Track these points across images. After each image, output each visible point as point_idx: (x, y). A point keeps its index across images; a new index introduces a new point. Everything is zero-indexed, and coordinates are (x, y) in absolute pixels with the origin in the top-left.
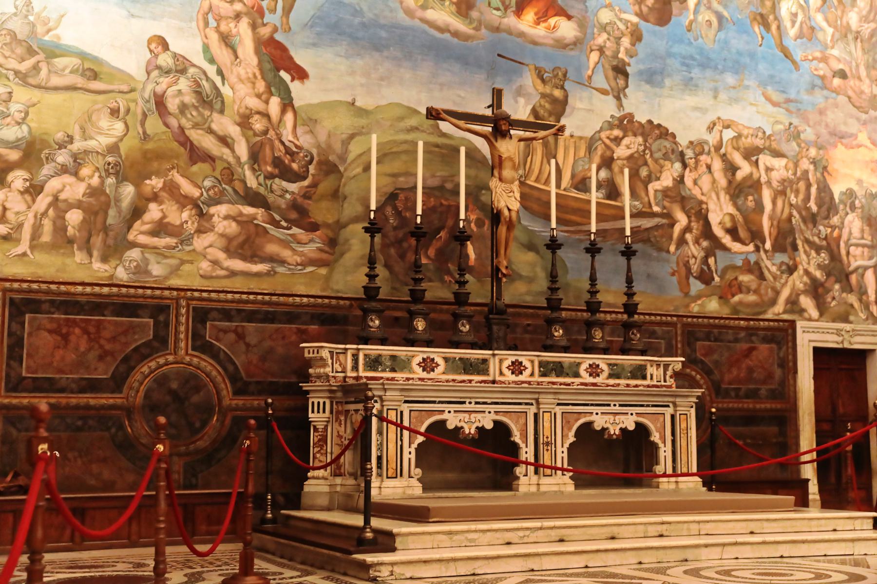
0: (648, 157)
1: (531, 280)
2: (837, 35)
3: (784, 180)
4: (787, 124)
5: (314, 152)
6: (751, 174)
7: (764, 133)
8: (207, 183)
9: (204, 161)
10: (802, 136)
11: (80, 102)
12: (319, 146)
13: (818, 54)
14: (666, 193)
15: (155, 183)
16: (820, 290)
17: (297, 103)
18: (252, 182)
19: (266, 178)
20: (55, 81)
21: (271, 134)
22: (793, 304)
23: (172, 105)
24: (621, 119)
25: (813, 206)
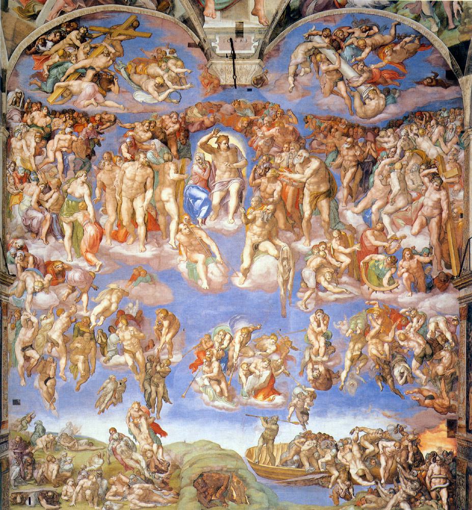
1: (260, 503)
4: (396, 425)
6: (374, 450)
8: (131, 477)
10: (405, 430)
11: (89, 454)
13: (416, 390)
14: (327, 463)
15: (114, 479)
16: (413, 500)
18: (147, 474)
20: (80, 448)
21: (154, 457)
23: (119, 451)
25: (410, 462)
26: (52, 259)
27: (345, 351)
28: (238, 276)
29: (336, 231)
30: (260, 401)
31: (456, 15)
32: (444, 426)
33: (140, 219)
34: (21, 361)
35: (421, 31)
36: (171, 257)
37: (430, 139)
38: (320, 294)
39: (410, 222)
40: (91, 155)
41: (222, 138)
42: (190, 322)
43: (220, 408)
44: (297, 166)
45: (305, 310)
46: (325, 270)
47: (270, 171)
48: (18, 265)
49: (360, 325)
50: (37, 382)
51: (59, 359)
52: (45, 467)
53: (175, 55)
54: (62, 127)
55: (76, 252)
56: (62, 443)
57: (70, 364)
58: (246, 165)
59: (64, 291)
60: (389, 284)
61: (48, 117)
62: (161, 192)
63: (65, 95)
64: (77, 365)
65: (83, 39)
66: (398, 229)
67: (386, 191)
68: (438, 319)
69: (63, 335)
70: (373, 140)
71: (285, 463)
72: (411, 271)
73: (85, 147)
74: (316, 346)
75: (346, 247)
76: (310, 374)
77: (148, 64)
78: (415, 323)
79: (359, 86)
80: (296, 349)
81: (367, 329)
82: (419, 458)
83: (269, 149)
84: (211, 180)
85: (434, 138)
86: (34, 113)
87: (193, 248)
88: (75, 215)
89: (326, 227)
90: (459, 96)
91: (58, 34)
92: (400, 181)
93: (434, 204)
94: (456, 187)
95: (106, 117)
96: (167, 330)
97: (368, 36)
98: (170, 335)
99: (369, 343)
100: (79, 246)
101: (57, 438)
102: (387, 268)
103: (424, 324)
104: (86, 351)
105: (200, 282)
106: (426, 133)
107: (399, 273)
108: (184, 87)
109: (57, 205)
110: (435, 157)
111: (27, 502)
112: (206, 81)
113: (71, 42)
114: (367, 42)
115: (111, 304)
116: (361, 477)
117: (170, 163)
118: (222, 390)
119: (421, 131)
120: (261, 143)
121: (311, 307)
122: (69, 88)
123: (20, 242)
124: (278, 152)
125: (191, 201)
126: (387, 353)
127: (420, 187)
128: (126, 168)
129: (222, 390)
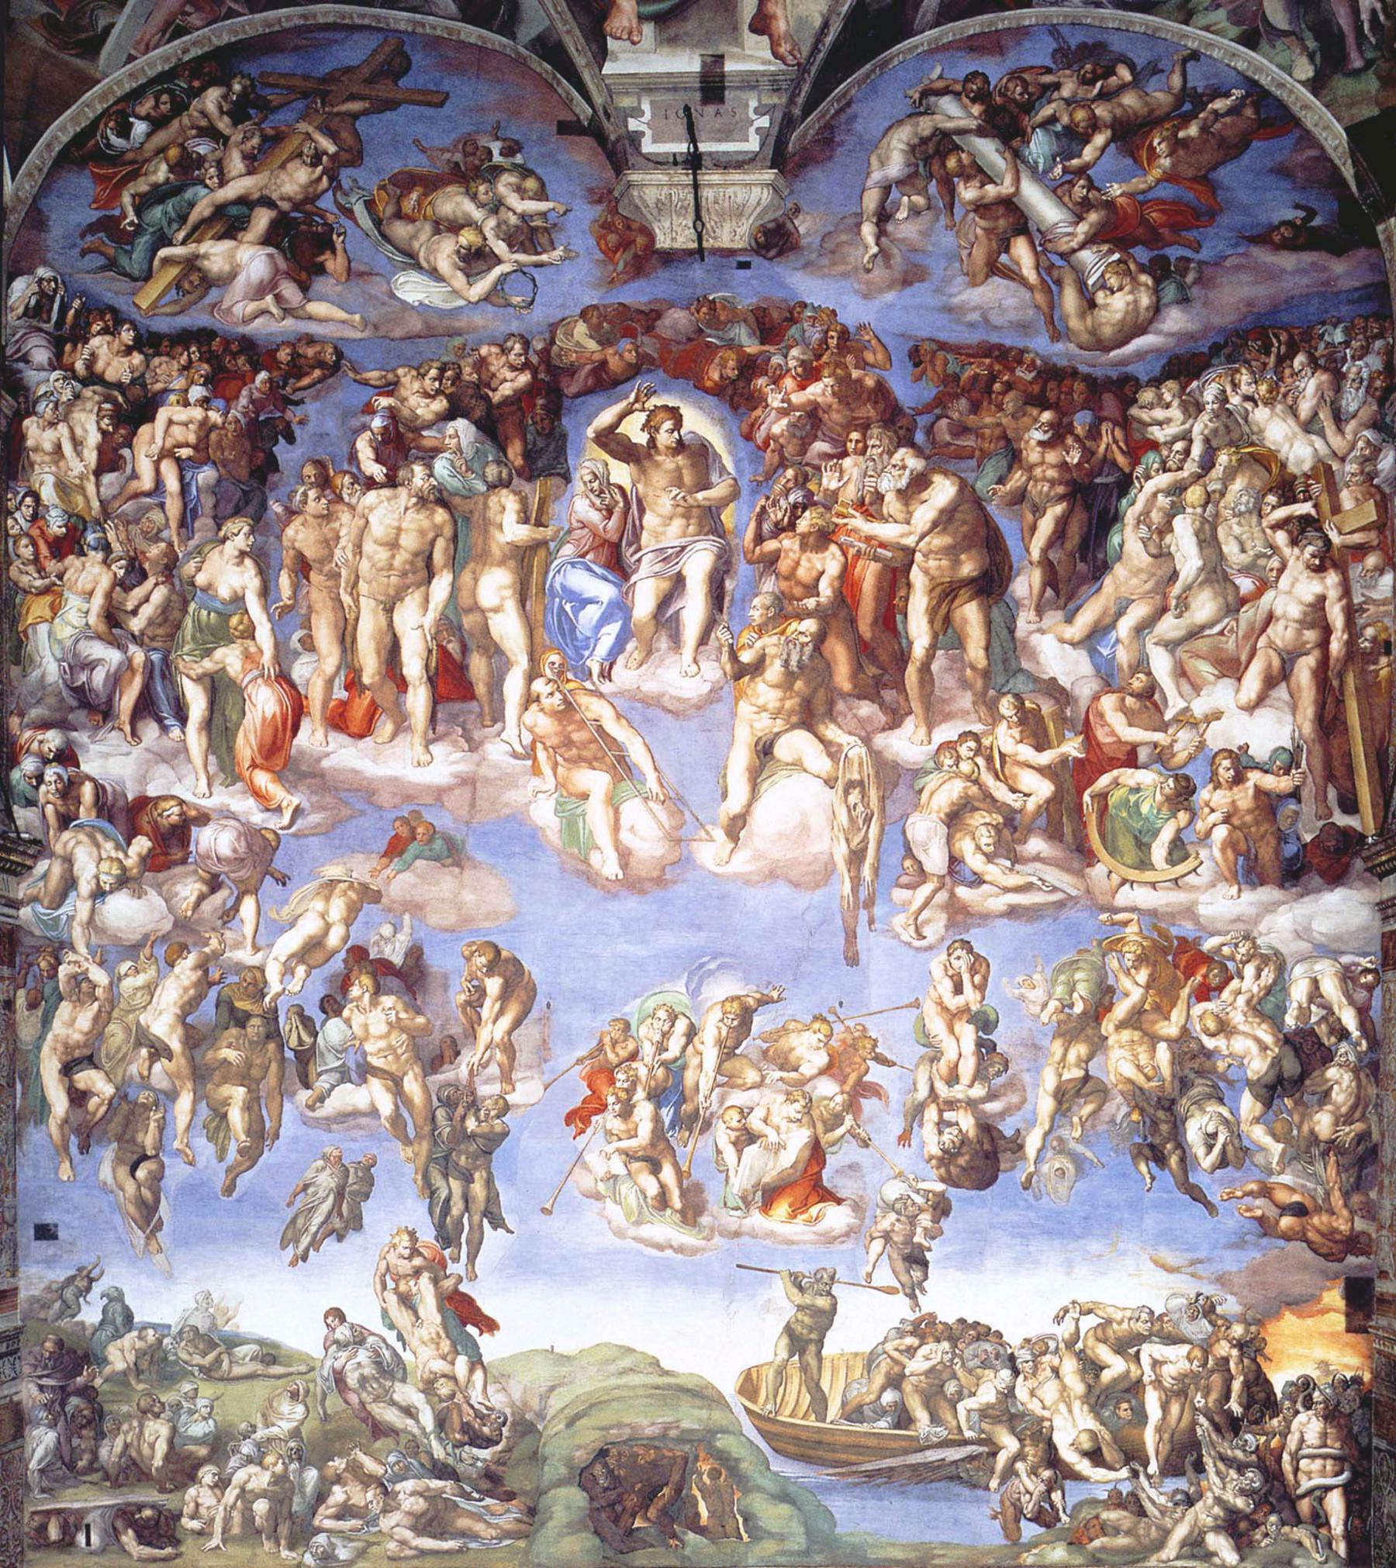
0: (957, 1367)
1: (781, 1538)
2: (1290, 1150)
3: (1185, 1376)
4: (1193, 1296)
5: (508, 1411)
6: (1128, 1372)
7: (1152, 1312)
8: (392, 1459)
9: (387, 1435)
10: (1219, 1310)
11: (260, 1390)
12: (512, 1404)
13: (1253, 1187)
14: (984, 1413)
15: (338, 1464)
16: (1243, 1525)
17: (486, 1360)
18: (438, 1452)
19: (455, 1446)
20: (238, 1371)
21: (459, 1396)
22: (1195, 1546)
23: (352, 1380)
24: (916, 1324)
26: (152, 791)
27: (1038, 1070)
28: (712, 840)
29: (1009, 697)
30: (778, 1221)
31: (1366, 27)
32: (1334, 1297)
33: (413, 666)
34: (59, 1102)
35: (1264, 81)
36: (509, 781)
37: (1293, 411)
38: (962, 892)
39: (1232, 668)
40: (265, 469)
41: (661, 415)
42: (566, 981)
43: (660, 1247)
44: (890, 497)
45: (917, 943)
46: (981, 821)
47: (807, 514)
48: (50, 809)
49: (1082, 989)
50: (106, 1163)
51: (172, 1095)
52: (131, 1428)
53: (519, 159)
54: (178, 383)
55: (222, 769)
56: (184, 1356)
57: (204, 1110)
58: (735, 495)
59: (188, 889)
60: (1172, 861)
61: (135, 354)
62: (476, 580)
63: (186, 286)
64: (225, 1116)
65: (238, 113)
66: (1197, 689)
67: (1160, 573)
68: (1318, 967)
69: (184, 1024)
70: (1116, 414)
71: (854, 1413)
72: (1236, 821)
73: (248, 445)
74: (950, 1054)
75: (1039, 748)
76: (931, 1141)
77: (436, 188)
78: (1250, 982)
79: (1074, 251)
80: (890, 1064)
81: (1104, 997)
82: (1262, 1395)
83: (804, 448)
84: (630, 545)
85: (1305, 408)
86: (95, 342)
87: (574, 751)
88: (219, 653)
89: (979, 684)
90: (1377, 279)
91: (165, 97)
92: (1201, 543)
93: (1305, 613)
94: (1372, 560)
95: (310, 352)
96: (497, 1006)
97: (1104, 96)
98: (506, 1022)
99: (1110, 1041)
100: (231, 749)
101: (166, 1341)
102: (1165, 811)
103: (1275, 983)
104: (255, 1072)
105: (595, 859)
106: (1279, 396)
107: (1200, 826)
108: (544, 257)
109: (165, 621)
110: (1307, 467)
111: (81, 1538)
112: (612, 238)
113: (204, 123)
114: (1098, 112)
115: (328, 927)
116: (1086, 1454)
117: (505, 491)
118: (663, 1187)
119: (1263, 388)
120: (779, 427)
121: (935, 929)
122: (198, 263)
123: (53, 739)
124: (830, 457)
125: (568, 607)
126: (1166, 1070)
127: (1262, 562)
128: (371, 509)
129: (663, 1187)
